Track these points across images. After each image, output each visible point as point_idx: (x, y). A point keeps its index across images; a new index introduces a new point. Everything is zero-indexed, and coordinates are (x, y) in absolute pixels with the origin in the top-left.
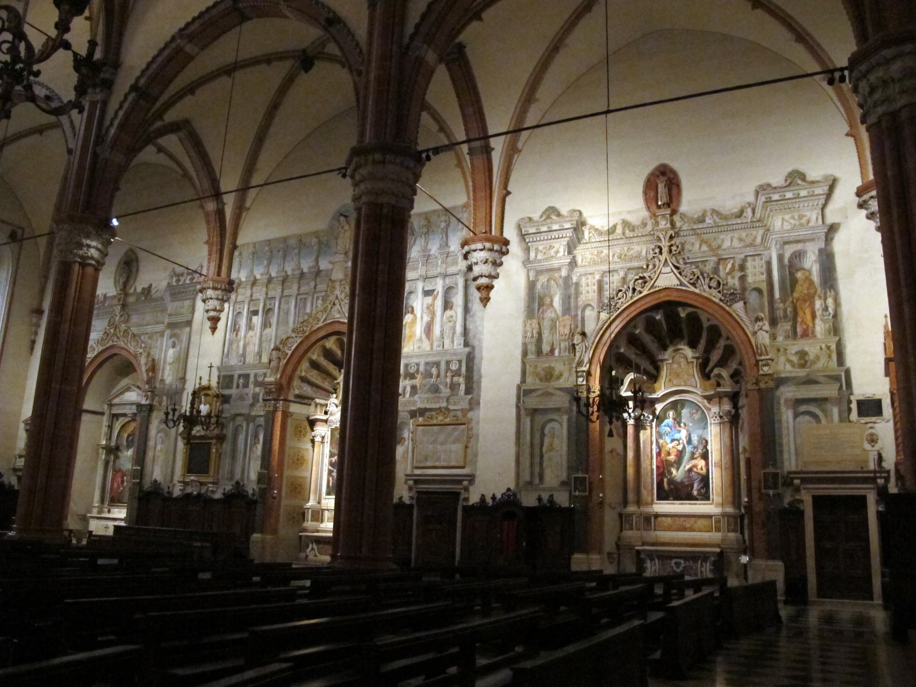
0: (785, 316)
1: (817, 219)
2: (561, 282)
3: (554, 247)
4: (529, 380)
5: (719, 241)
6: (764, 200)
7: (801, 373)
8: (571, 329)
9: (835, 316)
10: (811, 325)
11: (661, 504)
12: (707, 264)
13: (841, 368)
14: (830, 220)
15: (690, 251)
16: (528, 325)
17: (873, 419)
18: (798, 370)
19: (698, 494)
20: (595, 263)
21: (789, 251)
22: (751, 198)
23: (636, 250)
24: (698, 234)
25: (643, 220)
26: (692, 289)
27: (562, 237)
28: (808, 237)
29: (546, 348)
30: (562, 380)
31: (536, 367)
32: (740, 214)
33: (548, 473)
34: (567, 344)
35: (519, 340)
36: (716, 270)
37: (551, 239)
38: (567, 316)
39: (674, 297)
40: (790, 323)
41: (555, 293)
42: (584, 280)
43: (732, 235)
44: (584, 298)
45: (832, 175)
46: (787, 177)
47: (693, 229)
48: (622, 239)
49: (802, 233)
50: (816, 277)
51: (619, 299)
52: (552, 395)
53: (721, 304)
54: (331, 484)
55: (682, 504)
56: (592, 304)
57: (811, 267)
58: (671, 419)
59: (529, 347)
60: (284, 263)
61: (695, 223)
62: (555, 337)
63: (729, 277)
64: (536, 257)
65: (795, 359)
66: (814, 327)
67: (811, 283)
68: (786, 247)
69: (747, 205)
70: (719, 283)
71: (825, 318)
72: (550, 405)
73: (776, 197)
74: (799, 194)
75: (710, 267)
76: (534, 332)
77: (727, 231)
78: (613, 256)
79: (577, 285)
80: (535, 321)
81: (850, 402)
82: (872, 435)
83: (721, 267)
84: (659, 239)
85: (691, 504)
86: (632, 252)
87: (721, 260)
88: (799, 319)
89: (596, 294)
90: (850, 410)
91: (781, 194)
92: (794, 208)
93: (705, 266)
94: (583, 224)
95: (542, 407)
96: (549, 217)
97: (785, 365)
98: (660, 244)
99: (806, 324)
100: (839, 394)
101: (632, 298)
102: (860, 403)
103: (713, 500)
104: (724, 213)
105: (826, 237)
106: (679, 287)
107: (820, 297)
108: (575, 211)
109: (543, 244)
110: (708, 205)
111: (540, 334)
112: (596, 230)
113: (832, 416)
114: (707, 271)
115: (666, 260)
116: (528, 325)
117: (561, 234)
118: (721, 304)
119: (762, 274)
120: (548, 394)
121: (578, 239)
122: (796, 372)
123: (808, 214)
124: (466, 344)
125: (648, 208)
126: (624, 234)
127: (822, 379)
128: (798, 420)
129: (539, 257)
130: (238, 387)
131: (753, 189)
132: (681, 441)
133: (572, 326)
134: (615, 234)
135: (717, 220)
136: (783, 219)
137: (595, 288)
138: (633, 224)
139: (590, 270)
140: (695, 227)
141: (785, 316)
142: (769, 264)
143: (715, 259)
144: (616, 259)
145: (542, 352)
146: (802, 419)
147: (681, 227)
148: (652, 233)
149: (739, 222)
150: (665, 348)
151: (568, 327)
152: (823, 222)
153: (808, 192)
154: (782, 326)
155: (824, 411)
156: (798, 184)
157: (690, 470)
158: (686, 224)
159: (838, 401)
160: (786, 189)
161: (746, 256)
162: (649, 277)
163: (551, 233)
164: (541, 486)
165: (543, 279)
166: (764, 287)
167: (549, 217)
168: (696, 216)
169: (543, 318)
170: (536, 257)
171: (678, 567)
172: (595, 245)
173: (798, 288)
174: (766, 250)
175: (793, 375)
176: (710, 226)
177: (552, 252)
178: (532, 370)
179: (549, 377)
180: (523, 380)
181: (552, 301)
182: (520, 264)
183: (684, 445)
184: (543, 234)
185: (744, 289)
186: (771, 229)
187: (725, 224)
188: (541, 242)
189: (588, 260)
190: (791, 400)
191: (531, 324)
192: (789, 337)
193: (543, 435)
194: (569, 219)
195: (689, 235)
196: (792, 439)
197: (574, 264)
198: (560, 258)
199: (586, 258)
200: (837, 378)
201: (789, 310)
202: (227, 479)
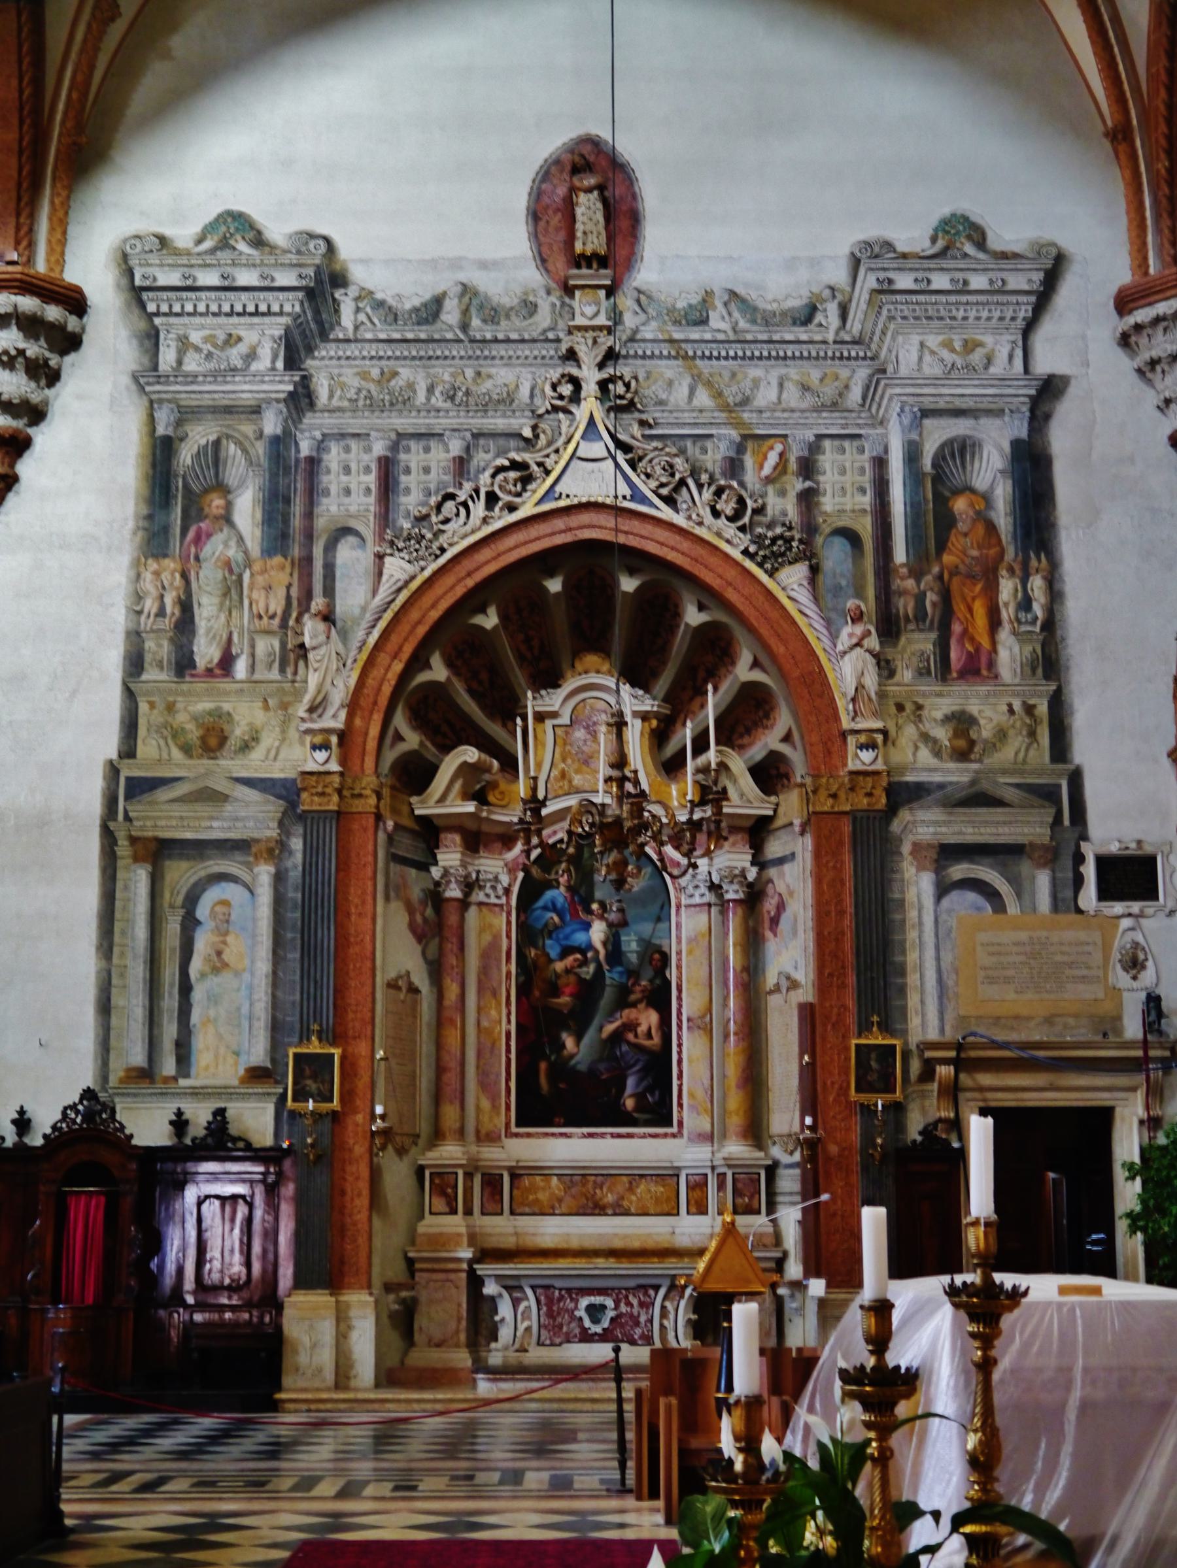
0: (920, 614)
1: (1011, 357)
2: (260, 449)
3: (240, 339)
4: (147, 748)
5: (747, 385)
6: (875, 285)
7: (956, 774)
8: (288, 598)
9: (1050, 625)
10: (985, 643)
11: (529, 1135)
12: (709, 444)
13: (1061, 766)
14: (1046, 362)
15: (661, 403)
16: (148, 576)
17: (1136, 907)
18: (952, 765)
19: (637, 1108)
20: (373, 405)
21: (937, 433)
22: (839, 275)
23: (500, 382)
24: (686, 357)
25: (526, 293)
26: (665, 512)
27: (269, 313)
28: (985, 404)
29: (206, 652)
30: (257, 754)
31: (170, 708)
32: (808, 315)
33: (203, 1045)
34: (276, 644)
35: (119, 619)
36: (734, 467)
37: (230, 314)
38: (278, 560)
39: (599, 529)
40: (934, 635)
41: (242, 484)
42: (333, 457)
43: (783, 371)
44: (334, 509)
45: (1054, 245)
46: (936, 230)
47: (671, 341)
48: (459, 341)
49: (967, 391)
50: (1002, 517)
51: (447, 521)
52: (224, 798)
53: (748, 564)
55: (591, 1135)
56: (361, 528)
57: (992, 487)
58: (562, 889)
59: (150, 645)
61: (677, 322)
62: (235, 620)
63: (770, 490)
64: (180, 362)
65: (942, 734)
66: (994, 650)
67: (991, 527)
68: (928, 423)
69: (827, 293)
70: (741, 501)
71: (1024, 628)
72: (217, 831)
73: (904, 281)
74: (966, 283)
75: (719, 457)
76: (169, 600)
77: (769, 357)
78: (431, 390)
79: (313, 464)
80: (170, 564)
81: (1079, 859)
82: (1136, 945)
83: (749, 461)
84: (571, 356)
85: (619, 1136)
86: (488, 385)
87: (749, 439)
88: (957, 628)
89: (372, 499)
90: (1079, 881)
91: (920, 275)
92: (953, 318)
93: (704, 451)
94: (339, 280)
95: (189, 835)
96: (224, 244)
97: (916, 748)
98: (575, 371)
99: (972, 640)
100: (1052, 838)
101: (485, 521)
102: (1105, 863)
103: (681, 1124)
104: (761, 305)
105: (1032, 410)
106: (626, 504)
107: (1011, 571)
108: (312, 236)
109: (203, 327)
110: (720, 278)
111: (186, 607)
112: (381, 304)
113: (1033, 894)
114: (710, 466)
115: (591, 421)
116: (148, 576)
117: (265, 301)
118: (748, 564)
119: (863, 491)
120: (211, 797)
121: (320, 323)
122: (948, 771)
123: (988, 339)
125: (543, 261)
126: (465, 327)
127: (1010, 794)
128: (946, 902)
129: (192, 364)
131: (846, 250)
132: (590, 955)
133: (294, 592)
134: (439, 325)
135: (742, 324)
136: (922, 344)
137: (371, 480)
138: (495, 300)
139: (353, 424)
141: (920, 614)
142: (880, 463)
143: (734, 434)
144: (438, 401)
145: (192, 664)
146: (955, 899)
147: (636, 331)
148: (551, 335)
149: (804, 337)
150: (549, 679)
151: (281, 593)
152: (1026, 370)
153: (991, 282)
154: (909, 641)
155: (1015, 882)
156: (966, 255)
157: (617, 1037)
158: (654, 324)
159: (1049, 856)
160: (932, 264)
161: (820, 437)
162: (540, 464)
163: (269, 295)
164: (183, 1082)
165: (200, 435)
166: (866, 527)
167: (224, 244)
168: (681, 305)
169: (197, 559)
170: (180, 362)
171: (596, 1321)
172: (373, 350)
173: (956, 541)
174: (873, 426)
175: (937, 778)
176: (721, 337)
177: (235, 354)
178: (157, 717)
179: (213, 742)
180: (128, 750)
181: (229, 506)
182: (126, 380)
183: (599, 967)
184: (203, 295)
185: (810, 528)
186: (890, 369)
187: (761, 337)
188: (197, 320)
189: (352, 394)
190: (930, 846)
191: (157, 574)
192: (929, 673)
193: (190, 923)
194: (294, 258)
195: (661, 357)
196: (930, 953)
197: (304, 402)
198: (259, 377)
199: (343, 386)
200: (1049, 794)
201: (931, 597)
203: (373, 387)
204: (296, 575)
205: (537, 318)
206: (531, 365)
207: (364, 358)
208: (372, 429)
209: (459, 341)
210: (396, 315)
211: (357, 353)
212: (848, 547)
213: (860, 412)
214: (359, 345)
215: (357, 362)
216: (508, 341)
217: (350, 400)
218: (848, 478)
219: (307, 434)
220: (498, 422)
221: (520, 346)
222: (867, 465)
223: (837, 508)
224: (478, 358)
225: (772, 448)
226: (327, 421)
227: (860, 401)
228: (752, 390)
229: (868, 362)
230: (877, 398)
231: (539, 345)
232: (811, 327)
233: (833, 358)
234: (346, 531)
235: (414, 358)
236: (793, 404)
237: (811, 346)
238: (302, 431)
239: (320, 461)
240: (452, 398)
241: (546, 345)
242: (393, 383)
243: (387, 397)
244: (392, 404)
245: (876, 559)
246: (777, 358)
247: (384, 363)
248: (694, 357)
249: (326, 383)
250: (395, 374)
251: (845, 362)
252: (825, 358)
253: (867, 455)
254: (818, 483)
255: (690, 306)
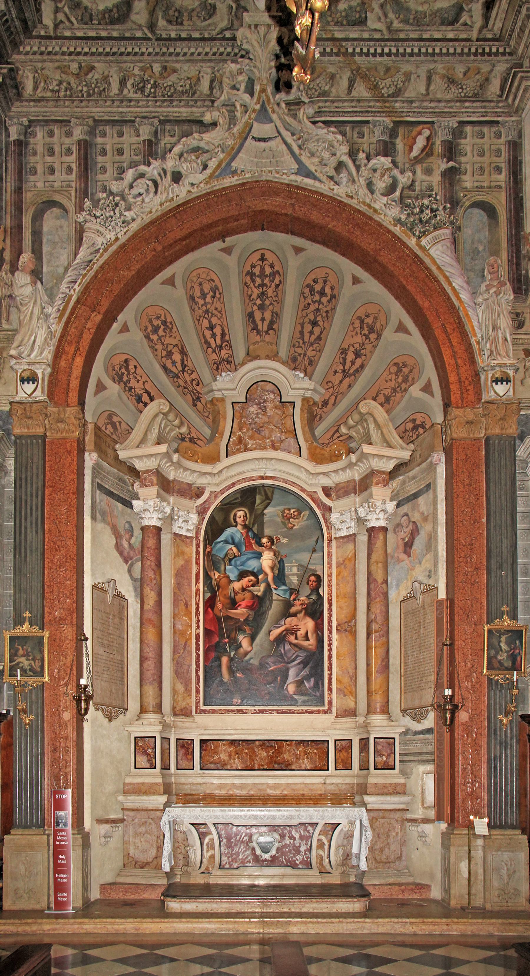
12: (365, 130)
24: (346, 54)
43: (432, 66)
47: (334, 39)
48: (149, 39)
78: (123, 82)
86: (173, 78)
89: (73, 177)
93: (361, 135)
119: (498, 170)
126: (152, 26)
132: (260, 577)
134: (129, 25)
135: (396, 24)
137: (72, 159)
140: (338, 35)
143: (388, 121)
144: (129, 92)
148: (228, 34)
149: (451, 35)
161: (462, 123)
176: (377, 36)
187: (412, 36)
189: (53, 86)
199: (46, 79)
203: (72, 80)
204: (8, 241)
205: (216, 19)
206: (210, 61)
207: (63, 53)
208: (72, 116)
209: (149, 39)
210: (91, 15)
211: (57, 49)
212: (485, 218)
213: (499, 102)
214: (60, 42)
215: (58, 57)
216: (190, 39)
217: (52, 91)
218: (486, 159)
219: (15, 120)
220: (184, 112)
221: (201, 44)
222: (503, 148)
223: (476, 184)
224: (164, 54)
225: (420, 133)
226: (33, 109)
227: (498, 93)
228: (404, 82)
229: (507, 57)
230: (513, 90)
231: (218, 43)
232: (457, 26)
233: (475, 54)
234: (52, 204)
235: (108, 54)
236: (439, 96)
237: (456, 44)
238: (11, 118)
239: (27, 144)
240: (142, 90)
241: (223, 43)
242: (90, 76)
243: (85, 89)
244: (89, 95)
245: (509, 229)
246: (427, 54)
247: (81, 58)
248: (353, 54)
249: (31, 76)
250: (92, 68)
251: (486, 57)
252: (469, 54)
253: (503, 140)
254: (460, 163)
255: (351, 8)
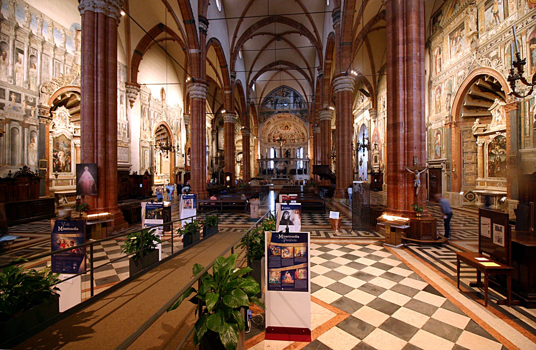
54: (55, 166)
60: (42, 30)
124: (127, 120)
130: (10, 99)
202: (9, 164)
